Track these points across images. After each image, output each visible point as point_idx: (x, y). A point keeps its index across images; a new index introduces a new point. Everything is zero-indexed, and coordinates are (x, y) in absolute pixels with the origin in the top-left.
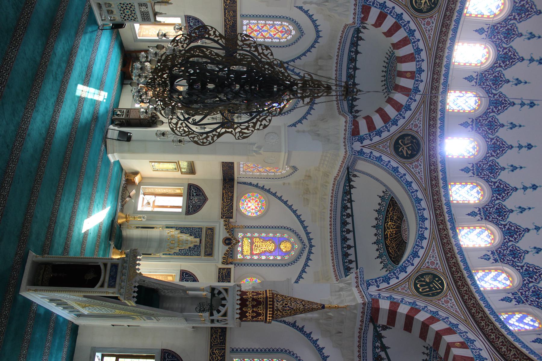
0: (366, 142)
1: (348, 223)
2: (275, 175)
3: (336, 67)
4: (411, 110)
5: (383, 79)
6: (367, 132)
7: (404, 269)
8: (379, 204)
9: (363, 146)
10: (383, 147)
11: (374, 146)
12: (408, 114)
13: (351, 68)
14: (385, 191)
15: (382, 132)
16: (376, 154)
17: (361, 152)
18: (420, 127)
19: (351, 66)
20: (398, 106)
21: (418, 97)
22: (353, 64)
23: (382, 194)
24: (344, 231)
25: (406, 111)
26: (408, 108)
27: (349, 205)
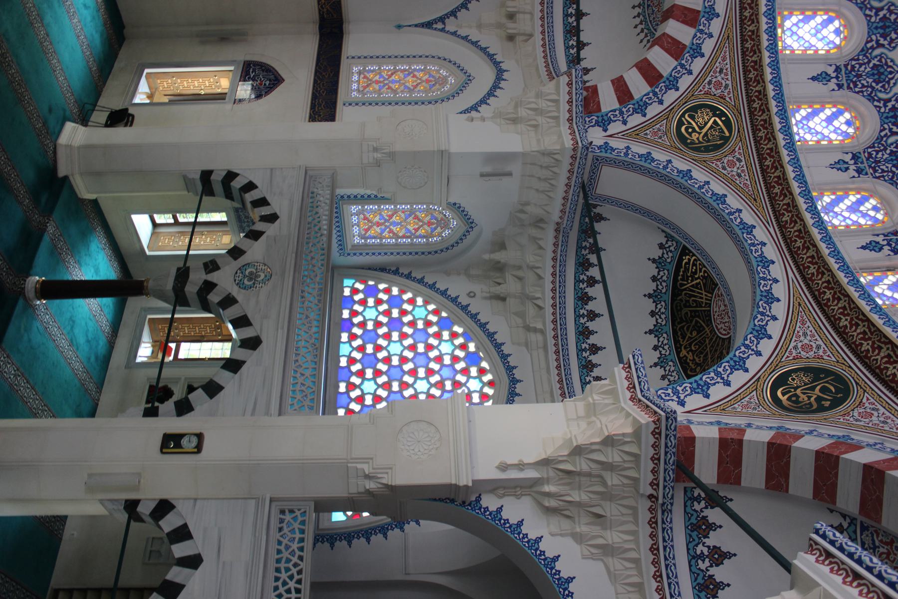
0: (615, 127)
1: (591, 265)
2: (428, 244)
3: (542, 11)
4: (703, 56)
5: (638, 20)
6: (617, 106)
7: (739, 364)
8: (654, 279)
9: (610, 136)
10: (655, 133)
11: (636, 134)
12: (698, 65)
13: (571, 15)
14: (664, 241)
15: (646, 105)
16: (639, 149)
17: (606, 147)
18: (726, 86)
19: (570, 10)
20: (675, 49)
21: (716, 26)
22: (575, 6)
23: (657, 253)
24: (585, 350)
25: (693, 57)
26: (697, 52)
27: (593, 259)
